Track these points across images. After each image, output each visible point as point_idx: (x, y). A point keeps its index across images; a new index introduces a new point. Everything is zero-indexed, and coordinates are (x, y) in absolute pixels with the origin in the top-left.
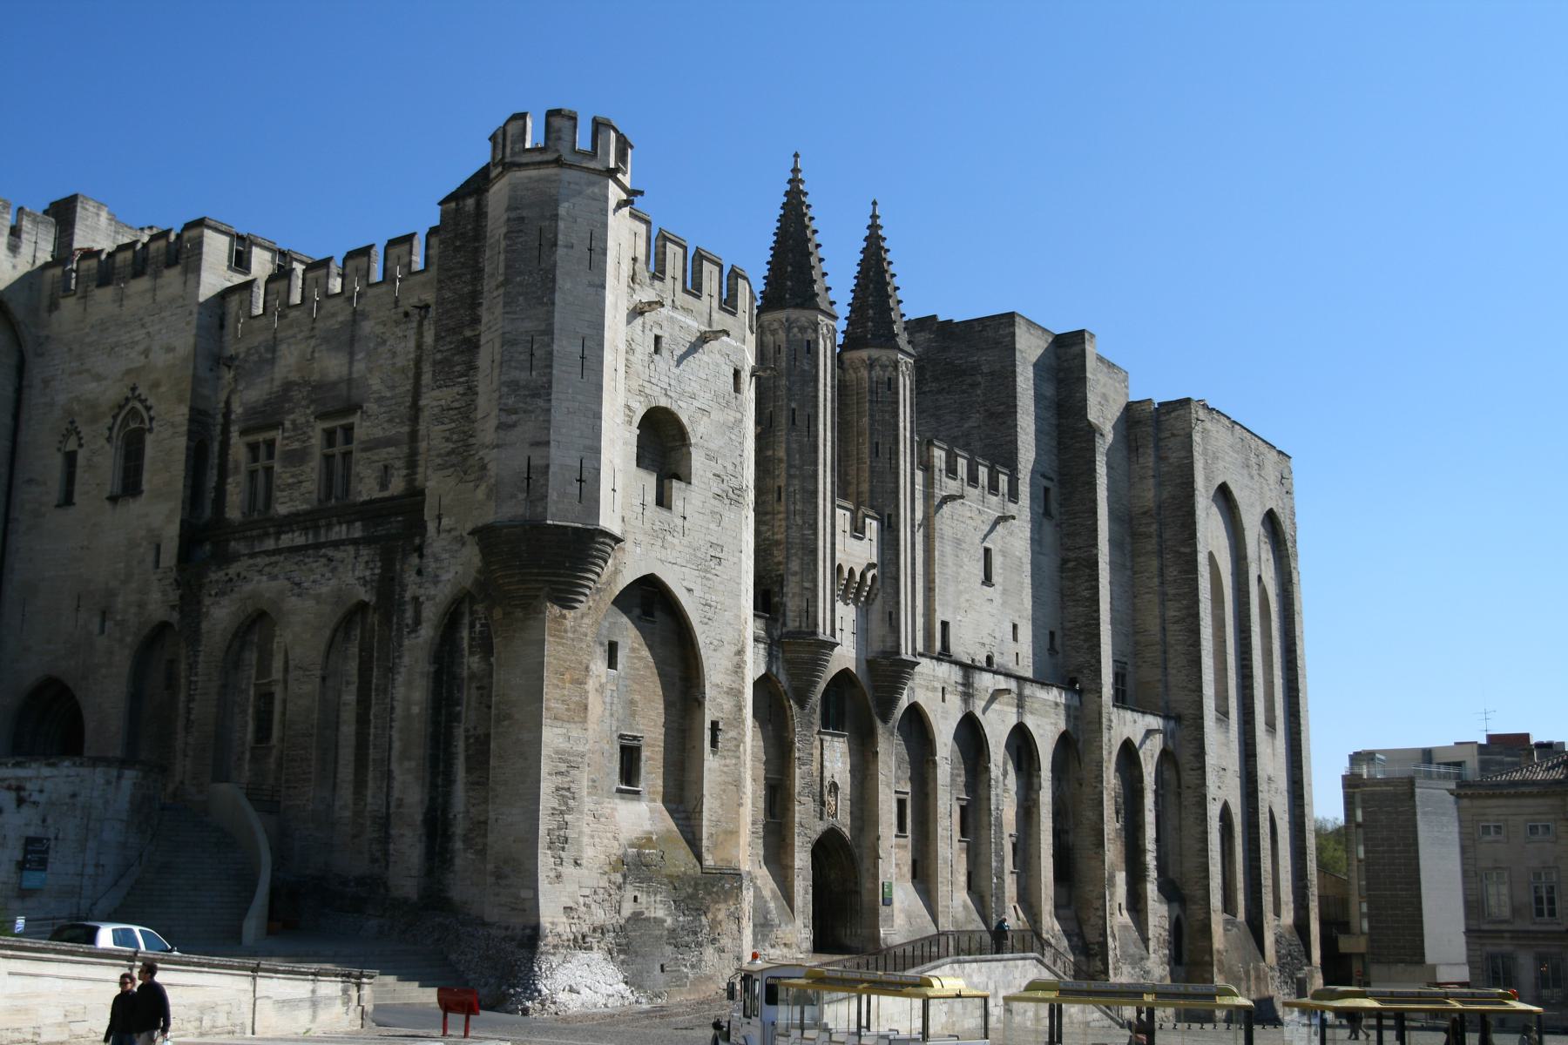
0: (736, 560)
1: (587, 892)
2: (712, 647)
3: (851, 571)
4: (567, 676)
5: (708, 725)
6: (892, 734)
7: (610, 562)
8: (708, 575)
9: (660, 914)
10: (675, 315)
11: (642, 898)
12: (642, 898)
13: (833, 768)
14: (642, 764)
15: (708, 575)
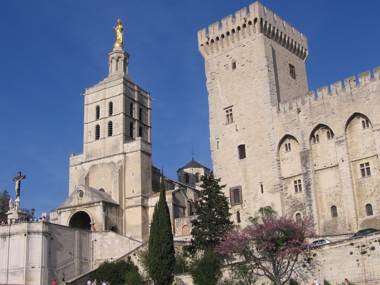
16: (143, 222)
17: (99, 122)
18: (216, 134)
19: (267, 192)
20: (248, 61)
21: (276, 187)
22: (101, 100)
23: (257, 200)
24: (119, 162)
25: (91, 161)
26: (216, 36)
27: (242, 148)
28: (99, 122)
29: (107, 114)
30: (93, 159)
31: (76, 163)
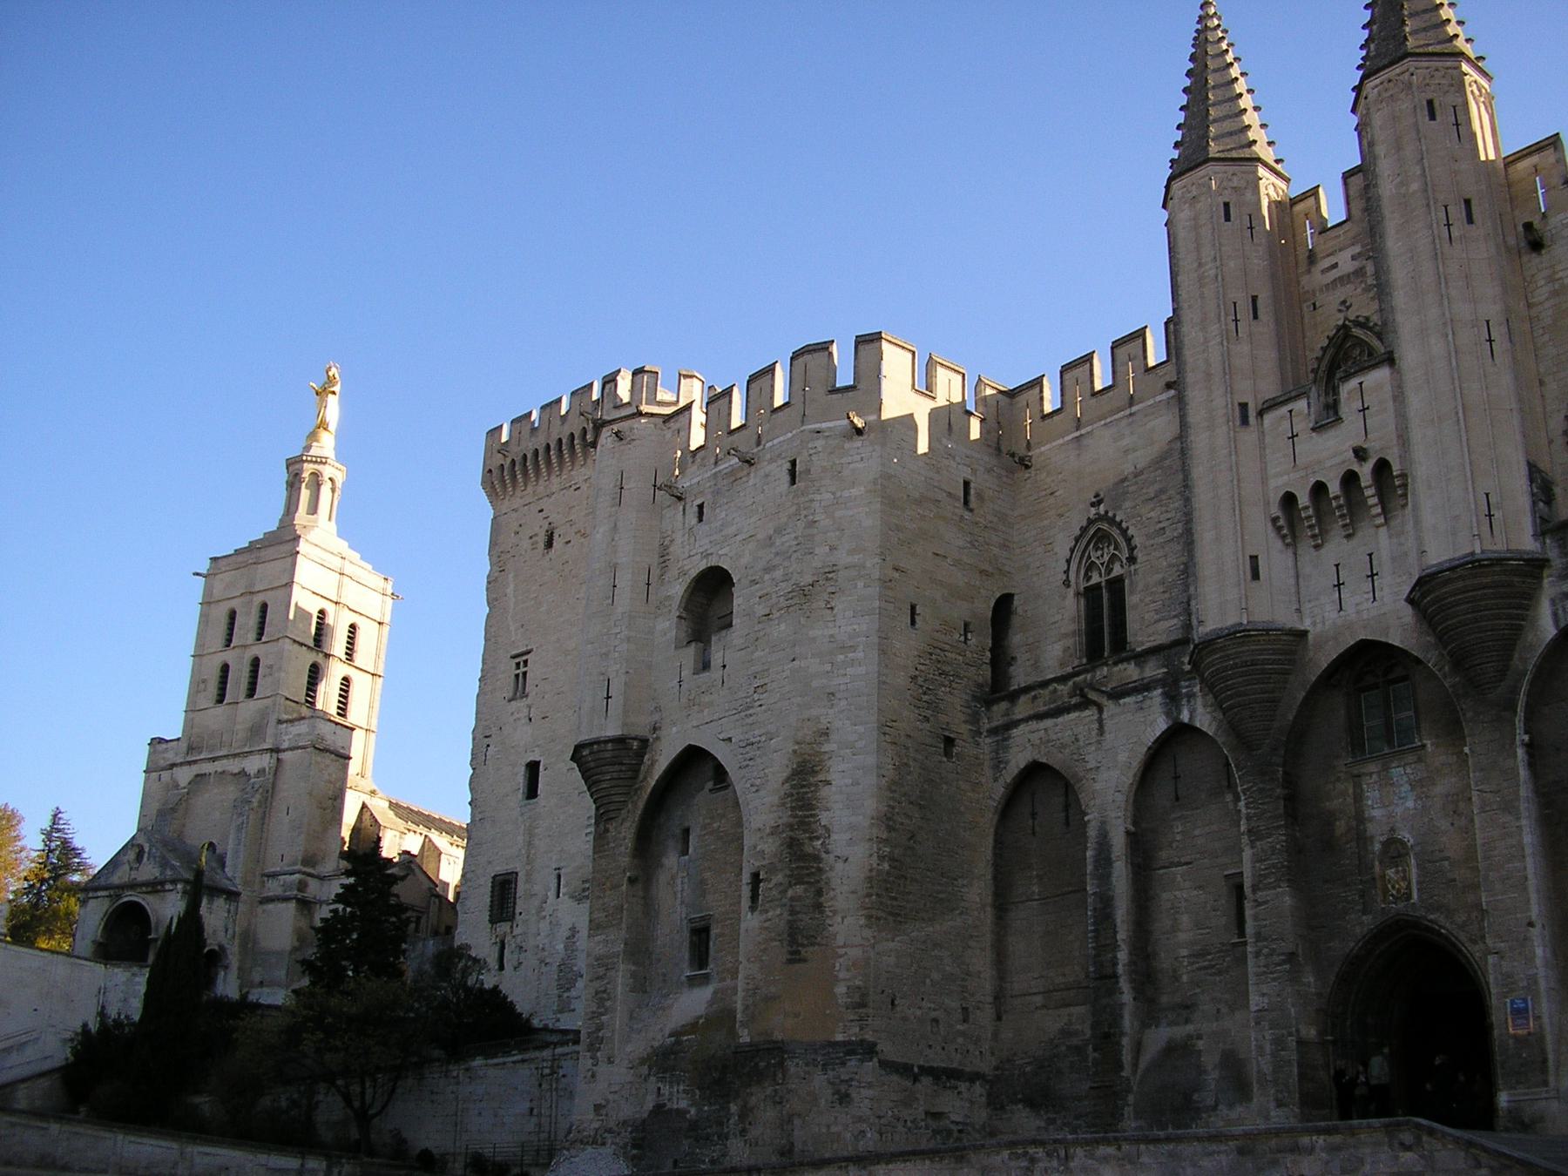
0: (787, 673)
1: (616, 1088)
2: (754, 789)
3: (1319, 489)
4: (608, 884)
5: (746, 877)
6: (1512, 708)
7: (646, 757)
8: (751, 711)
9: (683, 1104)
10: (717, 469)
11: (666, 1090)
12: (666, 1090)
13: (1390, 816)
14: (711, 944)
15: (751, 711)
16: (297, 944)
17: (229, 656)
18: (486, 723)
19: (566, 897)
20: (580, 531)
21: (587, 885)
22: (242, 595)
23: (544, 913)
24: (261, 772)
25: (195, 762)
26: (521, 450)
27: (533, 768)
28: (229, 656)
29: (252, 636)
30: (202, 757)
31: (162, 763)
